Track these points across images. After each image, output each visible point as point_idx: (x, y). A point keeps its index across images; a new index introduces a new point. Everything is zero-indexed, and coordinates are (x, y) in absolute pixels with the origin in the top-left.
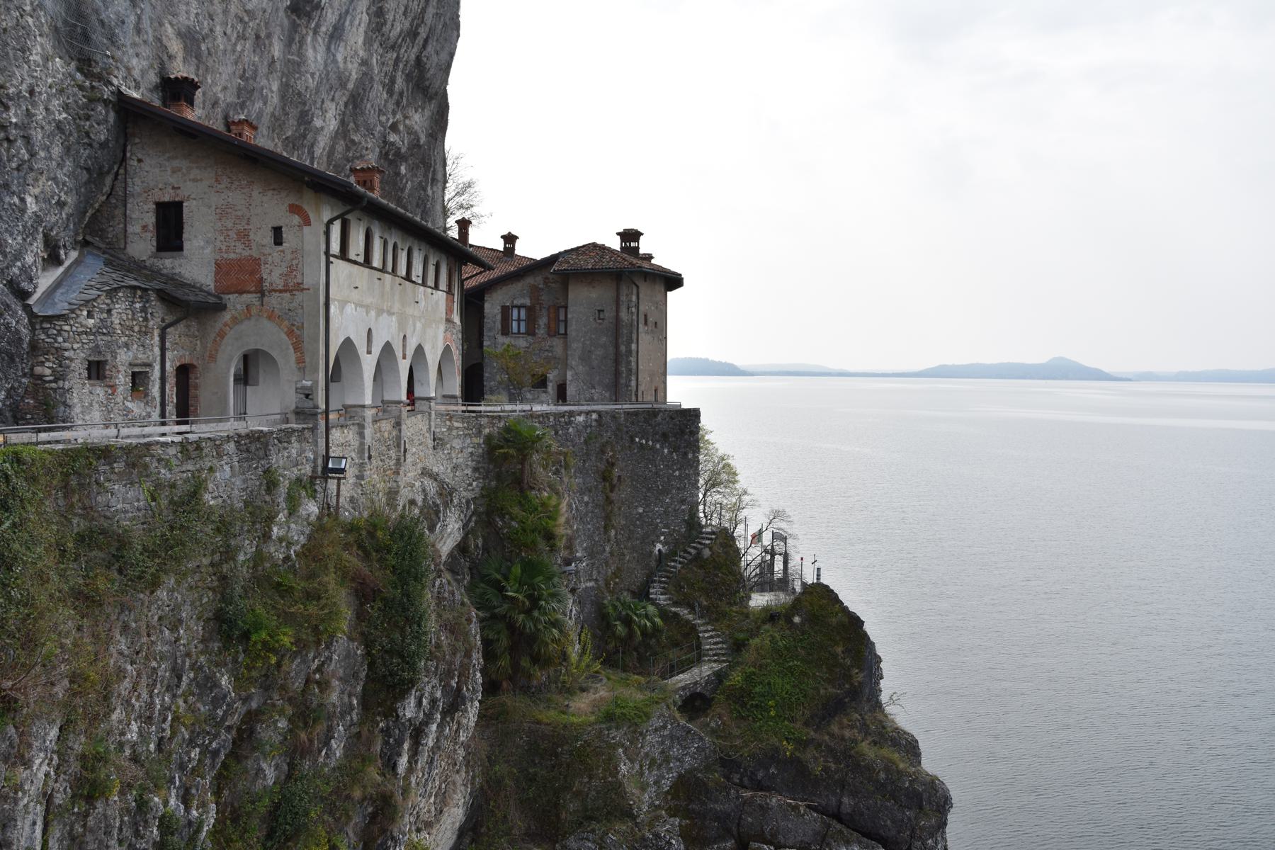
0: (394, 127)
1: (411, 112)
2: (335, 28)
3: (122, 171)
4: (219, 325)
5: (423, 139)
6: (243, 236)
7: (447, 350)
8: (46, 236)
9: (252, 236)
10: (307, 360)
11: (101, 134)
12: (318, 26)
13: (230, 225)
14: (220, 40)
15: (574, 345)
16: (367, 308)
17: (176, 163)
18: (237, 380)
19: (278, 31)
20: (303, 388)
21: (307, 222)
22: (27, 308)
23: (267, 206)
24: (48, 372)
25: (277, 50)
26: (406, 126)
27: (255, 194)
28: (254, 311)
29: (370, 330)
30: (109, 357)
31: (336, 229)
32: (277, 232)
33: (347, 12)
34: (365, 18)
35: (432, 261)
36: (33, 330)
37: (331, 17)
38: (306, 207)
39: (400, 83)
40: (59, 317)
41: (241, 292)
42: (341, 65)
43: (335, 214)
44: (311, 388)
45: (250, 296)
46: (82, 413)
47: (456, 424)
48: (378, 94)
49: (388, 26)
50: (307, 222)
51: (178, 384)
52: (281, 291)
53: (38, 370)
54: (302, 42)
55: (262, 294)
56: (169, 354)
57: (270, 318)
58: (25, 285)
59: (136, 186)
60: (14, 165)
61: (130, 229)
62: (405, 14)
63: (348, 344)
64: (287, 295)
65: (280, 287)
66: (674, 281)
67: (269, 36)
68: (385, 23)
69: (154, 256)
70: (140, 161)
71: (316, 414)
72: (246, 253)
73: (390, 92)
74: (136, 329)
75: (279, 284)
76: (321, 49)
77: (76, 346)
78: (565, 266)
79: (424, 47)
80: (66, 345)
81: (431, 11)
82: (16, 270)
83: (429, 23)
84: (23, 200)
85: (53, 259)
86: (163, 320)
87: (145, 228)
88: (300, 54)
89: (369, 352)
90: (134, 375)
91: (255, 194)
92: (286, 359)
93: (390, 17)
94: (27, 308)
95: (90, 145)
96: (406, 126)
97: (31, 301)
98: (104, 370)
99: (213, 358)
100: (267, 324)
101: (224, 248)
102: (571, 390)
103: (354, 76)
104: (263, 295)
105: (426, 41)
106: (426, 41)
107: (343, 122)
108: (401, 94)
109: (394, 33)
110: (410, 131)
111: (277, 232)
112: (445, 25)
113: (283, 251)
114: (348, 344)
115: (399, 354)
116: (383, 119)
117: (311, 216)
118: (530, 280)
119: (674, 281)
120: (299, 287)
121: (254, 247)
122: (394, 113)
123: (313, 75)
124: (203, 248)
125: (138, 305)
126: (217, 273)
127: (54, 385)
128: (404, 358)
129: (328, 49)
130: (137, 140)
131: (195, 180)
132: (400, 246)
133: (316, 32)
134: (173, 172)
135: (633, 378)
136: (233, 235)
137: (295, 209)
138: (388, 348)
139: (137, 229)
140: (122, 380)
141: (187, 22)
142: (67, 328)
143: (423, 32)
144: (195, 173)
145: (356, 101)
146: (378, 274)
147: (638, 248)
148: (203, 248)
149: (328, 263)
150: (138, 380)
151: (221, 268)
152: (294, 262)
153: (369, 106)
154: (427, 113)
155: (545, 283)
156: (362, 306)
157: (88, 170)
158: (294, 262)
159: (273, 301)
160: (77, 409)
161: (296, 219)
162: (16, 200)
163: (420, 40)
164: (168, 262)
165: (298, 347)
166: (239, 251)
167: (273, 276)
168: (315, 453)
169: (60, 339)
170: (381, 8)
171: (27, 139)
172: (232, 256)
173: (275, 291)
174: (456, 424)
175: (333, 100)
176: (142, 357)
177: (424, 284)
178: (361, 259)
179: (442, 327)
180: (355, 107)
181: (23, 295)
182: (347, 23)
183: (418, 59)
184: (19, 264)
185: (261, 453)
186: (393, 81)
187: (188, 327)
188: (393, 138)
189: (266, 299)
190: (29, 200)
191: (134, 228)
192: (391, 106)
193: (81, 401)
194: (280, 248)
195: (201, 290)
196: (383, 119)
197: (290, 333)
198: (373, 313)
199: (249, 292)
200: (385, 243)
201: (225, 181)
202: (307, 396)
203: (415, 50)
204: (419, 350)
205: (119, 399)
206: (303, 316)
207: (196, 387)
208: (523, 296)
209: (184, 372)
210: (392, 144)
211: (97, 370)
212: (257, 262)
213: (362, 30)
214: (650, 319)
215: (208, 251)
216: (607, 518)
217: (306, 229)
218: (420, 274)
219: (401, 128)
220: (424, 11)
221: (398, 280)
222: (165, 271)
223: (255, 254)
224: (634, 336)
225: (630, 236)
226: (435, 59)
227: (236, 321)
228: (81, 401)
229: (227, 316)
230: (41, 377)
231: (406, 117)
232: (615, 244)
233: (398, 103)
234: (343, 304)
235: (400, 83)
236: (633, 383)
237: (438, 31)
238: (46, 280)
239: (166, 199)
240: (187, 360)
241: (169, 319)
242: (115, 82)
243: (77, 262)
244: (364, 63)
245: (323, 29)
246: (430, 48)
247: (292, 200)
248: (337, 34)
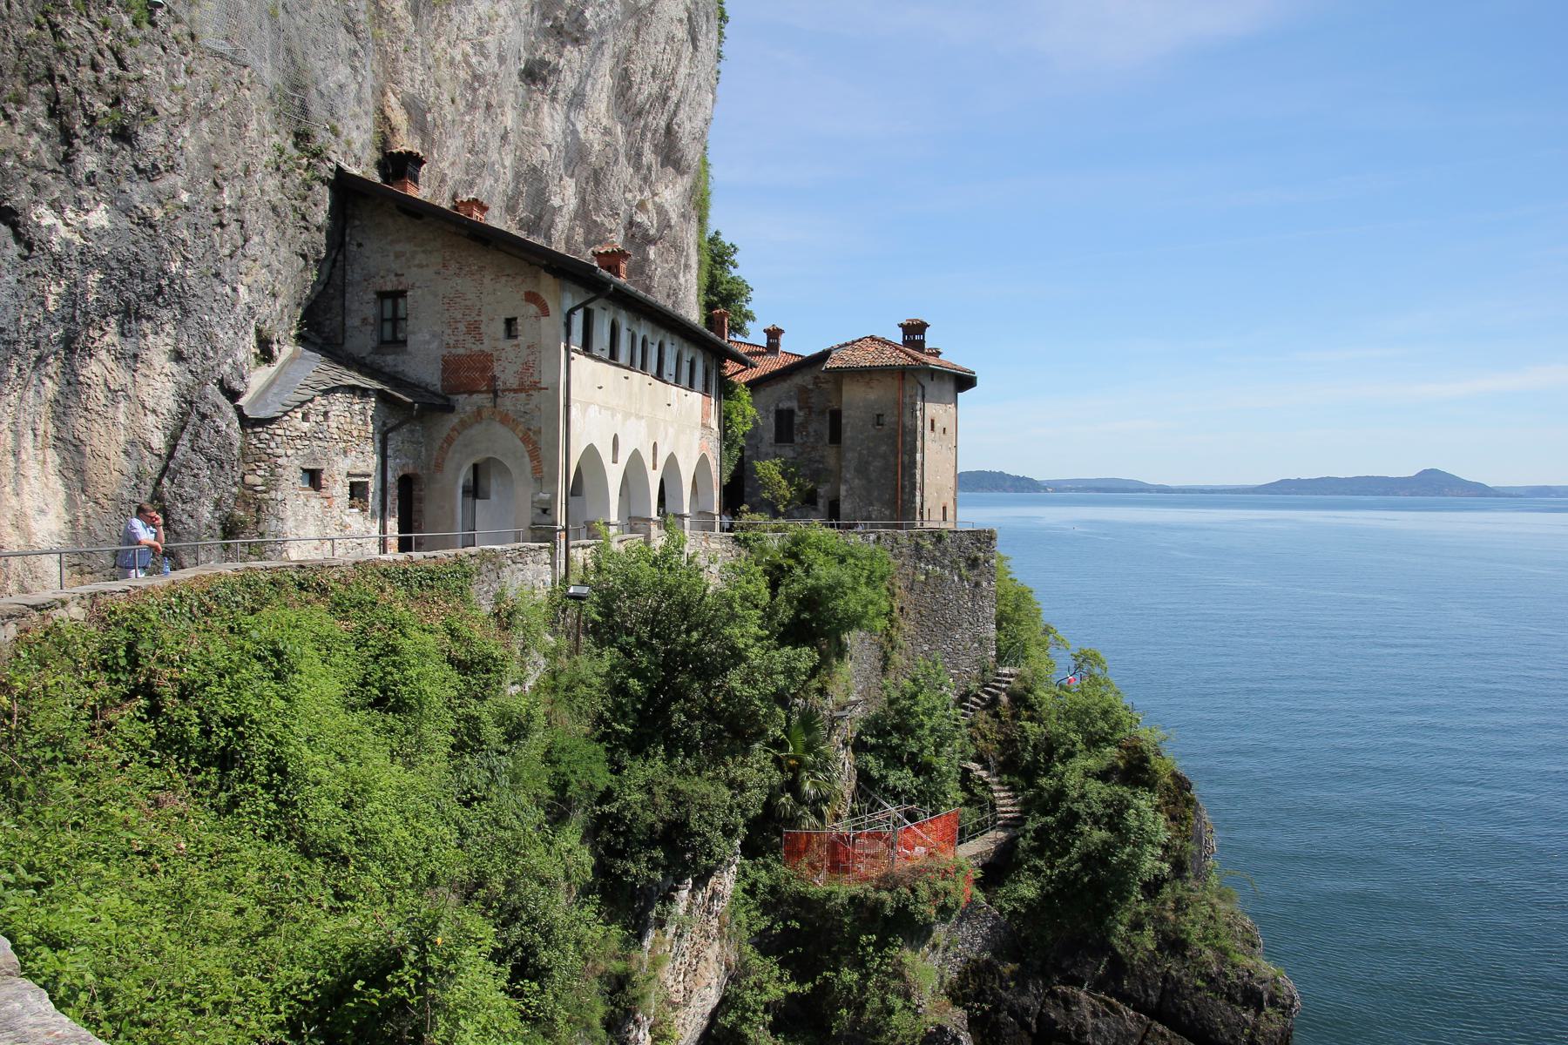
0: (641, 206)
1: (660, 188)
2: (575, 95)
3: (340, 257)
4: (445, 431)
5: (674, 218)
6: (474, 329)
7: (703, 460)
8: (259, 331)
9: (483, 328)
11: (321, 216)
12: (555, 92)
14: (448, 108)
15: (849, 455)
16: (613, 411)
17: (399, 248)
18: (466, 492)
19: (511, 98)
20: (541, 501)
21: (545, 312)
22: (239, 409)
23: (498, 295)
24: (259, 481)
25: (509, 119)
26: (654, 203)
27: (487, 281)
28: (485, 414)
29: (616, 439)
30: (325, 466)
31: (578, 320)
32: (510, 323)
33: (588, 75)
34: (608, 81)
35: (687, 357)
36: (245, 435)
37: (569, 81)
38: (544, 296)
39: (649, 157)
40: (272, 420)
41: (471, 393)
42: (582, 136)
43: (577, 303)
46: (296, 527)
47: (713, 546)
48: (624, 171)
49: (634, 90)
50: (545, 312)
51: (400, 497)
52: (515, 391)
53: (250, 479)
54: (537, 109)
55: (495, 393)
56: (390, 462)
58: (237, 385)
59: (355, 274)
60: (227, 252)
61: (349, 322)
62: (653, 74)
63: (591, 452)
64: (523, 395)
66: (964, 381)
67: (501, 105)
68: (630, 87)
69: (376, 351)
70: (360, 245)
71: (555, 531)
72: (476, 348)
73: (638, 167)
74: (355, 433)
75: (513, 382)
76: (560, 117)
77: (290, 452)
78: (838, 364)
79: (675, 114)
80: (280, 451)
81: (683, 71)
82: (226, 369)
83: (680, 85)
84: (234, 290)
85: (265, 353)
86: (384, 424)
87: (364, 321)
88: (536, 125)
89: (615, 462)
90: (352, 485)
91: (487, 281)
92: (521, 467)
93: (636, 79)
94: (239, 409)
95: (307, 229)
96: (654, 203)
97: (241, 402)
98: (320, 479)
99: (439, 466)
100: (500, 431)
101: (452, 342)
102: (845, 507)
103: (597, 147)
104: (496, 396)
105: (677, 105)
106: (677, 105)
107: (583, 200)
108: (649, 169)
109: (641, 98)
110: (661, 210)
111: (510, 323)
112: (699, 87)
114: (591, 452)
115: (649, 464)
116: (629, 196)
117: (550, 305)
118: (798, 380)
119: (964, 381)
120: (536, 386)
121: (486, 341)
122: (641, 191)
123: (549, 147)
124: (429, 343)
125: (357, 407)
126: (444, 371)
127: (266, 496)
128: (655, 467)
129: (567, 118)
130: (357, 223)
131: (420, 266)
132: (649, 339)
133: (553, 100)
134: (398, 256)
135: (918, 493)
136: (462, 327)
137: (532, 297)
138: (636, 457)
139: (356, 322)
140: (340, 490)
141: (411, 91)
142: (280, 432)
143: (674, 95)
144: (421, 258)
145: (597, 177)
146: (626, 372)
147: (923, 342)
148: (429, 343)
149: (569, 359)
150: (357, 491)
151: (451, 366)
153: (613, 182)
154: (679, 188)
155: (815, 383)
156: (607, 409)
157: (304, 257)
158: (531, 358)
159: (508, 403)
160: (290, 523)
161: (533, 309)
162: (228, 290)
163: (671, 106)
164: (390, 359)
165: (535, 454)
166: (469, 346)
167: (507, 374)
168: (554, 575)
169: (273, 445)
170: (626, 70)
171: (241, 223)
172: (461, 351)
174: (713, 546)
175: (572, 176)
176: (361, 467)
177: (677, 382)
178: (606, 355)
179: (698, 433)
180: (597, 182)
181: (233, 395)
182: (588, 87)
183: (669, 128)
184: (230, 361)
185: (493, 576)
186: (639, 155)
187: (412, 432)
188: (640, 218)
190: (242, 289)
191: (353, 321)
192: (637, 181)
193: (295, 514)
194: (515, 342)
195: (427, 390)
196: (629, 196)
197: (525, 440)
198: (619, 416)
200: (633, 338)
201: (453, 267)
202: (544, 511)
203: (665, 117)
204: (672, 461)
205: (336, 512)
206: (538, 418)
207: (420, 500)
208: (790, 398)
209: (407, 485)
210: (639, 225)
211: (314, 478)
213: (604, 95)
214: (937, 425)
215: (434, 345)
216: (886, 659)
217: (544, 320)
218: (673, 372)
219: (650, 206)
220: (674, 71)
221: (649, 379)
222: (387, 370)
223: (486, 346)
224: (919, 444)
225: (914, 332)
226: (687, 126)
227: (464, 425)
228: (295, 514)
229: (453, 420)
230: (252, 487)
231: (655, 195)
232: (897, 337)
233: (645, 179)
234: (586, 405)
235: (649, 157)
236: (918, 499)
237: (691, 94)
238: (259, 377)
239: (389, 288)
240: (410, 470)
241: (392, 422)
242: (334, 157)
243: (292, 359)
244: (607, 132)
245: (561, 95)
246: (682, 115)
247: (528, 286)
248: (577, 100)
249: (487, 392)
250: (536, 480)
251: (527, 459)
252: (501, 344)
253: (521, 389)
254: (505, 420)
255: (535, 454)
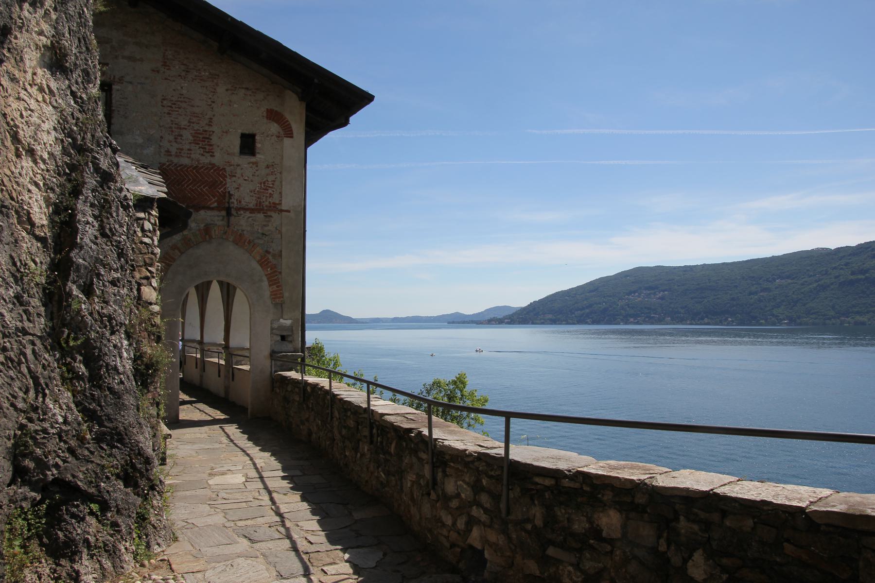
6: (203, 140)
9: (215, 139)
10: (286, 294)
13: (184, 123)
20: (282, 328)
38: (288, 116)
44: (291, 328)
45: (209, 213)
52: (252, 211)
57: (236, 242)
64: (261, 216)
65: (251, 206)
72: (206, 160)
75: (249, 200)
91: (221, 90)
101: (173, 150)
104: (229, 214)
113: (256, 164)
121: (217, 155)
131: (131, 59)
136: (187, 135)
137: (273, 116)
152: (270, 178)
158: (270, 178)
159: (243, 222)
161: (274, 128)
165: (274, 279)
172: (185, 161)
173: (245, 209)
189: (232, 219)
194: (253, 159)
199: (213, 209)
202: (283, 338)
212: (220, 172)
217: (287, 141)
223: (218, 159)
249: (218, 208)
250: (276, 305)
251: (265, 283)
252: (237, 159)
253: (258, 209)
254: (240, 240)
255: (274, 279)
